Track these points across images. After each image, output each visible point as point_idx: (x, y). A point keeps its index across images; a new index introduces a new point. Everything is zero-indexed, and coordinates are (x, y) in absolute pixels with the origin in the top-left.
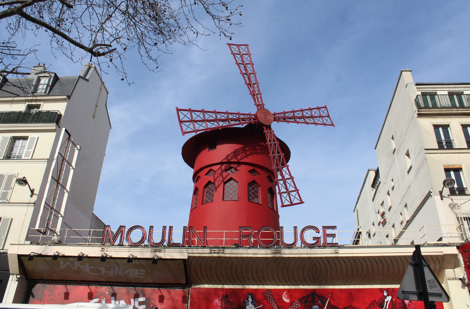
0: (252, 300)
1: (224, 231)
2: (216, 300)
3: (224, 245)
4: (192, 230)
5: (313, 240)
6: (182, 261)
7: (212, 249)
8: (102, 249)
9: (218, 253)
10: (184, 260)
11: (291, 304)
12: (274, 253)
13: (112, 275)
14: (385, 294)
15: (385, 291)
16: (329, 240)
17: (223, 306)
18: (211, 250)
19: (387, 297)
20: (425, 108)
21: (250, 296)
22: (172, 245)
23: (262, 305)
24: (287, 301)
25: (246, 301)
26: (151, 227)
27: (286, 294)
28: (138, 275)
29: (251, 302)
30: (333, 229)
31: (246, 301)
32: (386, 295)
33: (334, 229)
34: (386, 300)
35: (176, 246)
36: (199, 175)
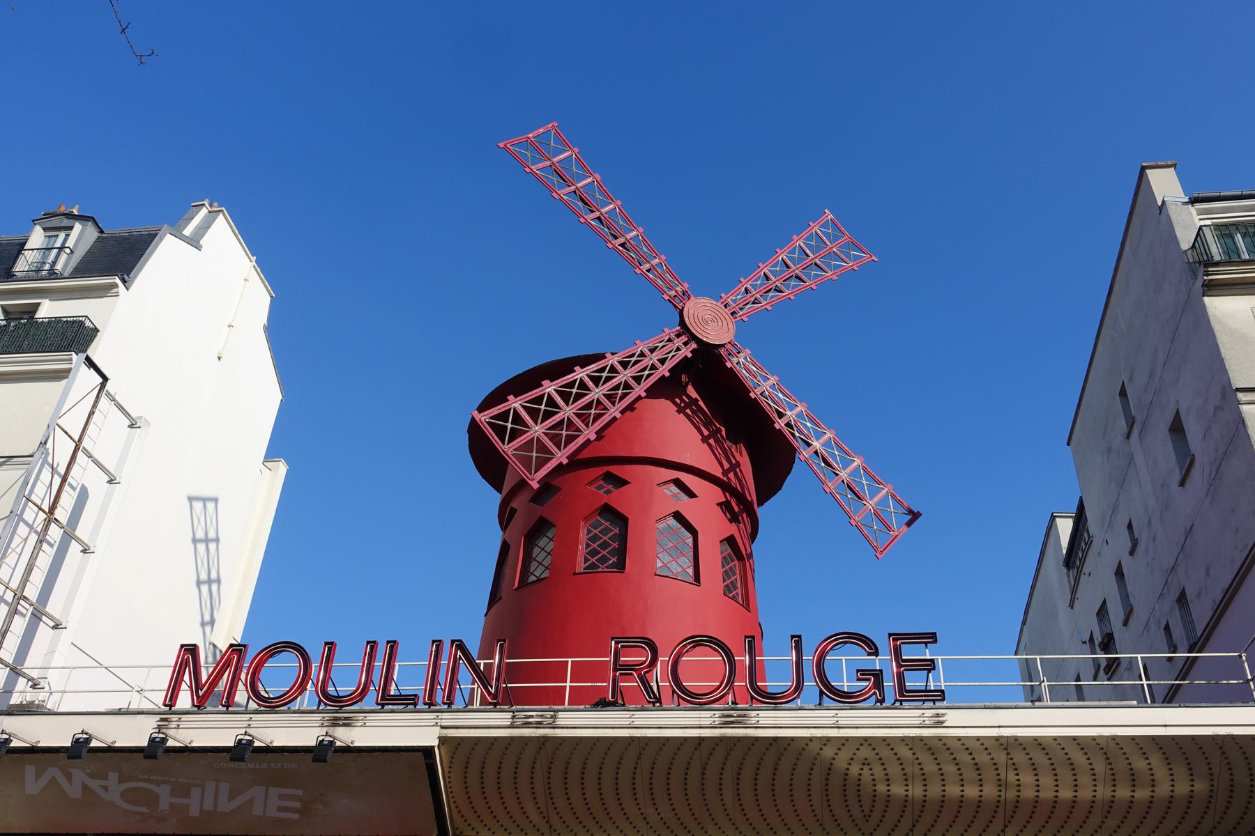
1: (570, 660)
3: (569, 704)
4: (459, 653)
5: (859, 680)
6: (420, 754)
7: (516, 713)
8: (162, 720)
9: (539, 725)
10: (427, 752)
12: (725, 725)
13: (194, 812)
16: (914, 681)
18: (514, 717)
20: (1229, 262)
22: (389, 701)
26: (331, 645)
28: (281, 809)
30: (926, 643)
33: (928, 645)
35: (408, 702)
36: (514, 505)
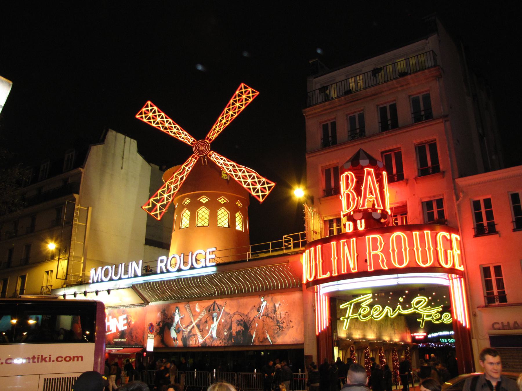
0: (178, 312)
2: (158, 313)
11: (200, 313)
14: (262, 300)
15: (263, 298)
17: (163, 317)
19: (264, 302)
21: (177, 309)
23: (184, 315)
24: (198, 310)
25: (175, 312)
27: (198, 305)
29: (178, 313)
31: (175, 312)
32: (263, 301)
34: (262, 305)
